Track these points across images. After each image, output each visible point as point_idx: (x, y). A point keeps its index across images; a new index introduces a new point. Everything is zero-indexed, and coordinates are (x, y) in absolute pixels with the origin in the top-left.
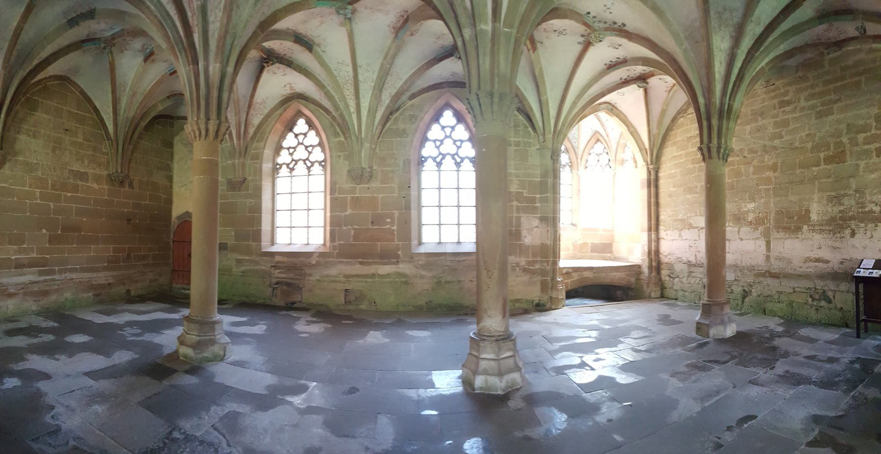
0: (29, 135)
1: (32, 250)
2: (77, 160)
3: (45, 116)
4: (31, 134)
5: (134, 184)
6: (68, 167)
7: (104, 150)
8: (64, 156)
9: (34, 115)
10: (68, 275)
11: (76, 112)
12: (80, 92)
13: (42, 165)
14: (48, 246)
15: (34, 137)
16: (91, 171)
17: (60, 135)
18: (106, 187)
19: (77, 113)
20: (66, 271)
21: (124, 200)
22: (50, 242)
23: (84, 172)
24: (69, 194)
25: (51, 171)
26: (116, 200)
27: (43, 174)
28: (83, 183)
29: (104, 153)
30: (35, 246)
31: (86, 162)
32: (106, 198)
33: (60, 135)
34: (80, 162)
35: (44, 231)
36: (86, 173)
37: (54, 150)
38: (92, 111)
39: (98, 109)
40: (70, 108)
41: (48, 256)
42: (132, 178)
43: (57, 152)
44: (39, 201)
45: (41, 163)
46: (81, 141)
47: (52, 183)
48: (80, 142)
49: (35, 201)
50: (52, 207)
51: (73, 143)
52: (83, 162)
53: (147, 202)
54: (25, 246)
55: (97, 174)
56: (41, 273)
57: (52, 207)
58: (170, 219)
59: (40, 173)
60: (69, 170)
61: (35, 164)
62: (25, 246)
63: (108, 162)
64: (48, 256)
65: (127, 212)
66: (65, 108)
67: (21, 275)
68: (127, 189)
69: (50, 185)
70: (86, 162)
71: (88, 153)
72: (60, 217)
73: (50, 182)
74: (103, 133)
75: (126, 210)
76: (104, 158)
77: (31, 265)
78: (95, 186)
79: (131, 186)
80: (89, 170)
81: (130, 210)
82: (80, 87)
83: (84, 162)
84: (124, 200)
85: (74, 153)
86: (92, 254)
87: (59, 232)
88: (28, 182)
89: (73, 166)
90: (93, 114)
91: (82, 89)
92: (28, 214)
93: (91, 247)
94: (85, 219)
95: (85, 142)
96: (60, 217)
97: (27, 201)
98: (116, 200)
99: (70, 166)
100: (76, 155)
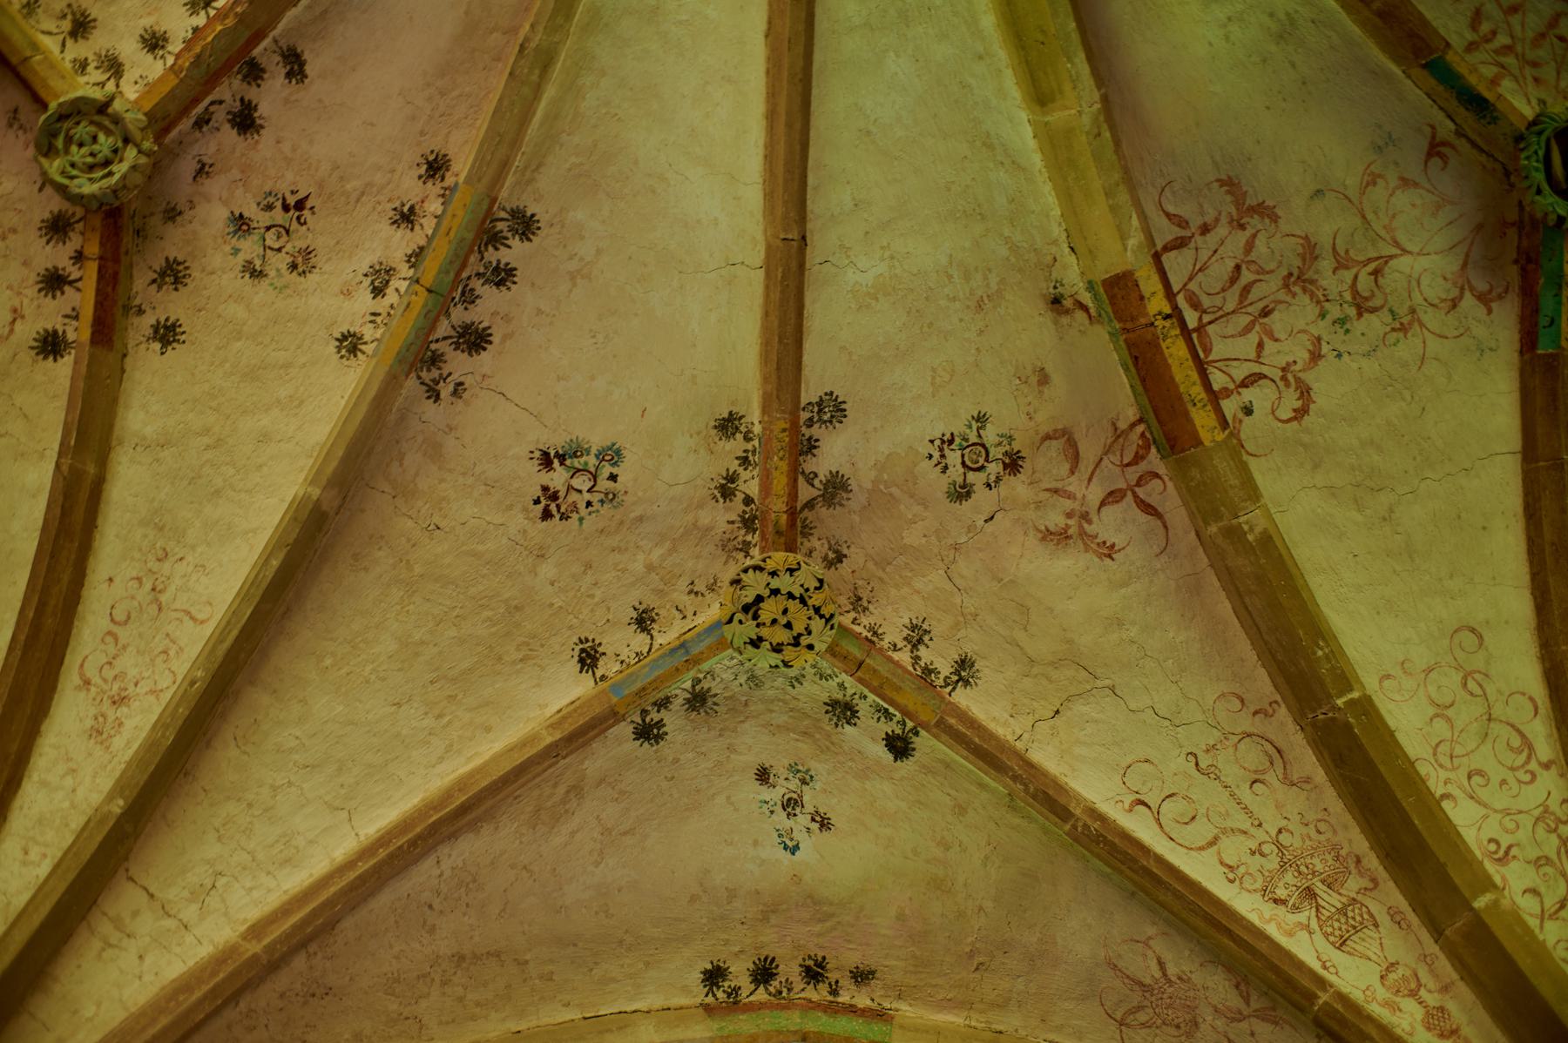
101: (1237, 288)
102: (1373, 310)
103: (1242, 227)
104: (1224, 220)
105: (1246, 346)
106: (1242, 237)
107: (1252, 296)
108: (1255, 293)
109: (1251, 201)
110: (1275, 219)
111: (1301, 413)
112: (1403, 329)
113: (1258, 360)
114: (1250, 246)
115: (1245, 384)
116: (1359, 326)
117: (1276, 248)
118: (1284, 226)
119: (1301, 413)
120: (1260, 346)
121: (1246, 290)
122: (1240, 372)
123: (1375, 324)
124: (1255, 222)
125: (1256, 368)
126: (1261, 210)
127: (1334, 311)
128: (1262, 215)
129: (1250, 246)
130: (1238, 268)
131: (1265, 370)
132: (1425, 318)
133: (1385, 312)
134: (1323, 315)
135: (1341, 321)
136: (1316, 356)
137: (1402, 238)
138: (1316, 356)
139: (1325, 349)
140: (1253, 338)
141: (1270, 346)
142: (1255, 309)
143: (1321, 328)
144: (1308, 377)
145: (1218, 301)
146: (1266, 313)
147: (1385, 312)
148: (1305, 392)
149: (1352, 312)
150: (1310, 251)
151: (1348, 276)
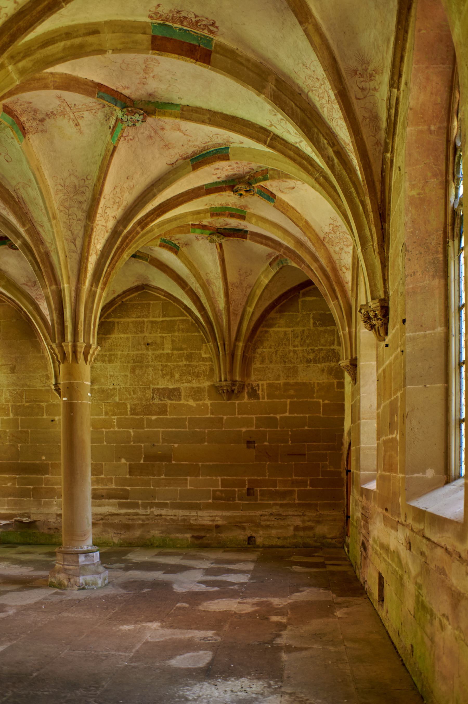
0: (104, 361)
1: (110, 480)
2: (163, 377)
3: (122, 335)
4: (106, 359)
5: (260, 392)
6: (152, 386)
7: (204, 356)
8: (146, 375)
9: (109, 338)
10: (156, 511)
11: (161, 319)
12: (164, 296)
13: (120, 389)
14: (128, 476)
15: (110, 361)
16: (184, 386)
17: (140, 352)
18: (208, 402)
19: (162, 321)
20: (152, 505)
21: (240, 416)
22: (130, 473)
23: (174, 389)
24: (154, 418)
25: (130, 395)
26: (225, 417)
27: (120, 399)
28: (174, 402)
29: (204, 360)
30: (113, 477)
31: (177, 376)
32: (209, 416)
33: (140, 352)
34: (168, 377)
35: (123, 461)
36: (178, 390)
37: (133, 370)
38: (185, 312)
39: (189, 309)
40: (154, 317)
41: (129, 488)
42: (255, 384)
43: (137, 372)
44: (116, 429)
45: (118, 387)
46: (170, 352)
47: (131, 408)
48: (168, 354)
49: (112, 430)
50: (132, 434)
51: (158, 357)
52: (172, 376)
53: (287, 414)
54: (103, 476)
55: (193, 388)
56: (121, 506)
57: (132, 434)
58: (342, 436)
59: (117, 399)
60: (154, 389)
61: (111, 390)
62: (103, 476)
63: (212, 370)
64: (129, 488)
65: (246, 432)
66: (146, 320)
67: (99, 506)
68: (246, 400)
69: (129, 409)
70: (177, 376)
71: (180, 364)
72: (143, 445)
73: (129, 406)
74: (202, 333)
75: (244, 430)
76: (204, 365)
77: (110, 497)
78: (192, 403)
79: (253, 394)
80: (182, 385)
81: (254, 429)
82: (162, 290)
83: (174, 377)
84: (240, 416)
85: (160, 368)
86: (189, 488)
87: (142, 461)
88: (104, 410)
89: (158, 384)
90: (186, 316)
91: (166, 292)
92: (105, 443)
93: (186, 480)
94: (176, 445)
95: (175, 352)
96: (143, 445)
97: (103, 429)
98: (225, 417)
99: (154, 384)
100: (162, 370)
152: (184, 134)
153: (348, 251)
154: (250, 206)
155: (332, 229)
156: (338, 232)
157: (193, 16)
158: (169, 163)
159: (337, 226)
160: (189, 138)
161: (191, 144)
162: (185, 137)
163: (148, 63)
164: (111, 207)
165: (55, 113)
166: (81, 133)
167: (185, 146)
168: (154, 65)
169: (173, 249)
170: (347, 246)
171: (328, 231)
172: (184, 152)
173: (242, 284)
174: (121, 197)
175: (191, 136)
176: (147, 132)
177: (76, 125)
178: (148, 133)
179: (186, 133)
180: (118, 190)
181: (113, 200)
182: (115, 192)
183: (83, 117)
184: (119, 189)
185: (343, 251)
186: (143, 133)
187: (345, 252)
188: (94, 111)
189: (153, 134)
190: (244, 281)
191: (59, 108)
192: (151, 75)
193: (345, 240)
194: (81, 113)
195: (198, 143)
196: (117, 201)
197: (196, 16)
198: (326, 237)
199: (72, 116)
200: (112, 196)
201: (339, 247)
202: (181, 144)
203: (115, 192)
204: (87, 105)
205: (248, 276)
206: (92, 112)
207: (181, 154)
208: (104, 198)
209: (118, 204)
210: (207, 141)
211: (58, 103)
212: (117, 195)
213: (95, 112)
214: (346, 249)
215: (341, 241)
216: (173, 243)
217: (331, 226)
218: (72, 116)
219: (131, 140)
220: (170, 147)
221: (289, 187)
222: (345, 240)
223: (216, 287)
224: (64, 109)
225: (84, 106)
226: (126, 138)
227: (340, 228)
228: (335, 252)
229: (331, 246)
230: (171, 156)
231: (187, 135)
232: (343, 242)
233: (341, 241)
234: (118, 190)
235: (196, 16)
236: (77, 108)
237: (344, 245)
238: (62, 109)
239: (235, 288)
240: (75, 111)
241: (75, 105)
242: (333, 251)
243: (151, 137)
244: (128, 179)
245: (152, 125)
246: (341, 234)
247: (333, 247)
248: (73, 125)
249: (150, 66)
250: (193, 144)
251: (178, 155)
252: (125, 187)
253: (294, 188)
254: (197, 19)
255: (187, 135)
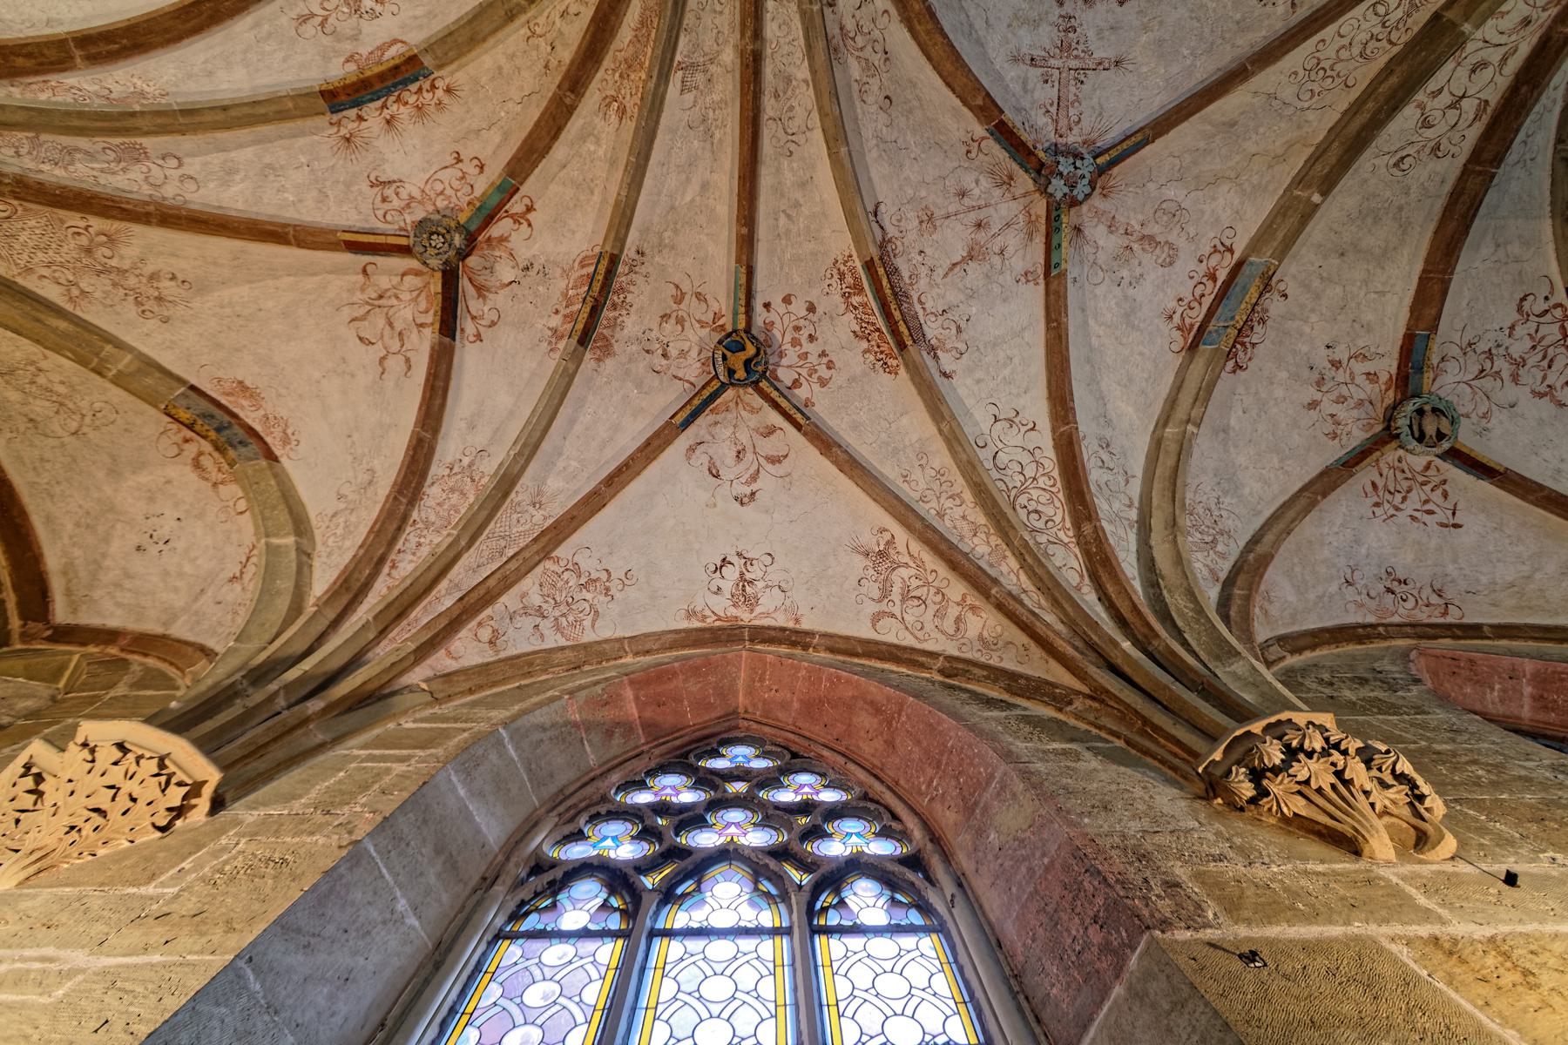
101: (1549, 358)
102: (1484, 352)
103: (1549, 386)
104: (1559, 388)
105: (1544, 330)
106: (1548, 382)
107: (1541, 354)
108: (1540, 356)
109: (1547, 399)
110: (1533, 392)
111: (1523, 299)
112: (1470, 345)
113: (1539, 324)
114: (1544, 378)
115: (1547, 311)
116: (1490, 345)
117: (1531, 377)
118: (1527, 389)
119: (1523, 299)
120: (1537, 331)
121: (1544, 357)
122: (1548, 317)
123: (1482, 346)
124: (1543, 389)
125: (1542, 320)
126: (1541, 395)
127: (1502, 351)
128: (1539, 393)
129: (1544, 378)
130: (1550, 367)
131: (1537, 319)
132: (1459, 350)
133: (1479, 351)
134: (1507, 348)
135: (1499, 346)
136: (1512, 328)
137: (1468, 390)
138: (1512, 328)
139: (1507, 332)
140: (1540, 335)
141: (1532, 332)
142: (1539, 348)
143: (1507, 342)
144: (1517, 316)
145: (1558, 351)
146: (1534, 347)
147: (1479, 351)
148: (1520, 309)
149: (1493, 351)
150: (1515, 378)
151: (1495, 369)
152: (955, 265)
153: (546, 632)
154: (609, 363)
155: (594, 576)
156: (589, 596)
157: (1254, 341)
158: (882, 208)
159: (608, 589)
160: (940, 272)
161: (924, 271)
162: (947, 264)
163: (1166, 248)
164: (858, 13)
165: (1071, 35)
166: (1016, 59)
167: (920, 258)
168: (1158, 257)
169: (357, 91)
170: (558, 628)
171: (583, 566)
172: (900, 248)
173: (99, 273)
174: (860, 54)
175: (946, 275)
176: (976, 192)
177: (1032, 59)
178: (974, 192)
179: (957, 269)
180: (877, 59)
181: (865, 30)
182: (878, 48)
183: (1046, 82)
184: (876, 63)
185: (539, 620)
186: (977, 182)
187: (536, 626)
188: (1053, 110)
189: (967, 201)
190: (115, 285)
191: (1081, 47)
192: (1135, 246)
193: (571, 619)
194: (1056, 84)
195: (923, 283)
196: (859, 39)
197: (1254, 345)
198: (562, 563)
199: (1052, 62)
200: (876, 34)
201: (545, 606)
202: (928, 251)
203: (878, 48)
204: (1076, 104)
205: (138, 303)
206: (1051, 105)
207: (898, 243)
208: (886, 11)
209: (852, 34)
210: (926, 306)
211: (1098, 55)
212: (869, 48)
213: (1048, 111)
214: (546, 626)
215: (563, 608)
216: (372, 100)
217: (604, 576)
218: (1052, 62)
219: (969, 152)
220: (924, 225)
221: (718, 464)
222: (571, 619)
223: (102, 171)
224: (1076, 57)
225: (1072, 97)
226: (976, 144)
227: (602, 598)
228: (524, 595)
229: (537, 582)
230: (899, 221)
231: (951, 269)
232: (564, 615)
233: (563, 608)
234: (877, 59)
235: (1254, 345)
236: (1073, 82)
237: (556, 619)
238: (1075, 53)
239: (84, 241)
240: (1064, 75)
241: (1082, 82)
242: (525, 589)
243: (963, 194)
244: (887, 97)
245: (991, 209)
246: (586, 605)
247: (537, 587)
248: (1036, 53)
249: (1158, 251)
250: (923, 275)
251: (897, 234)
252: (871, 81)
253: (717, 476)
254: (1248, 345)
255: (951, 269)
